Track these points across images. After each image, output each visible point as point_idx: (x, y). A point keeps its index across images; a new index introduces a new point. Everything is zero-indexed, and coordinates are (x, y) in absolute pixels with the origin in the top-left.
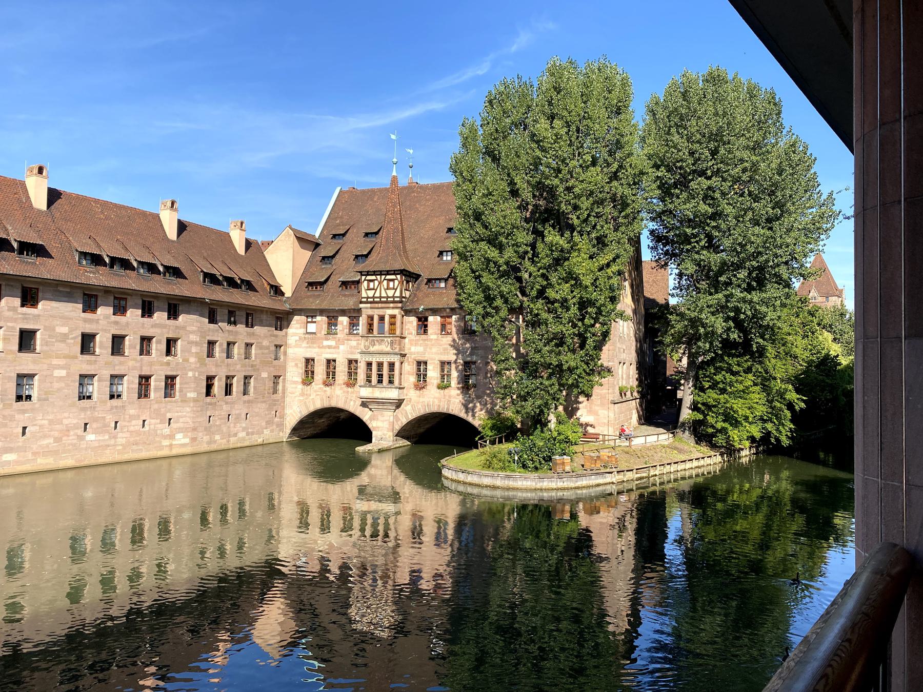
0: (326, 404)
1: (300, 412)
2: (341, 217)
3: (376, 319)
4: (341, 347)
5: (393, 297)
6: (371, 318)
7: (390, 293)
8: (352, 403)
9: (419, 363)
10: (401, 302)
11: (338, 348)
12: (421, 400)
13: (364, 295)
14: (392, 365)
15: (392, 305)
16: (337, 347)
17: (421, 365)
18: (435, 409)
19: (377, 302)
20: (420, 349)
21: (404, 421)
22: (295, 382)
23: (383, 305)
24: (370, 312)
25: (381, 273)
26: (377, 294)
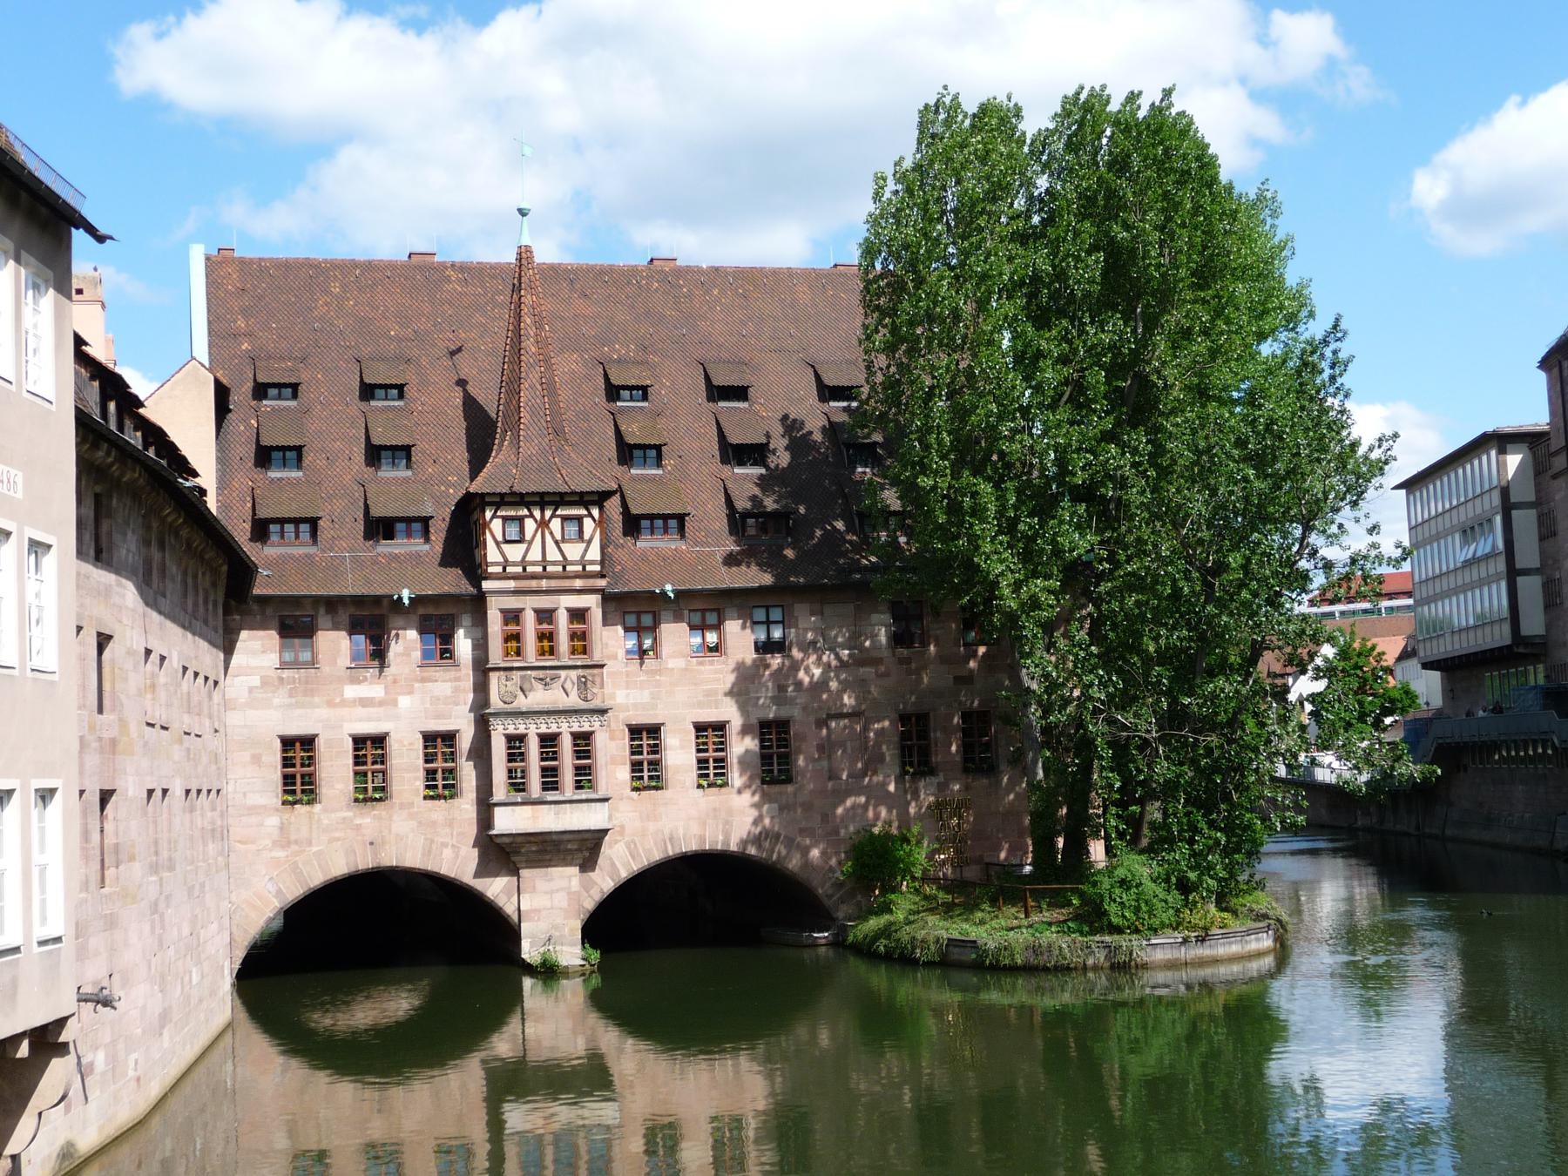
0: (365, 861)
1: (279, 892)
2: (249, 335)
3: (529, 619)
4: (404, 702)
6: (512, 616)
7: (573, 551)
8: (447, 853)
9: (635, 731)
10: (603, 576)
11: (395, 703)
12: (652, 827)
13: (492, 554)
14: (583, 741)
15: (578, 583)
16: (389, 702)
17: (645, 736)
18: (692, 846)
19: (534, 576)
20: (644, 696)
22: (253, 810)
23: (554, 584)
24: (512, 603)
25: (545, 500)
26: (535, 554)
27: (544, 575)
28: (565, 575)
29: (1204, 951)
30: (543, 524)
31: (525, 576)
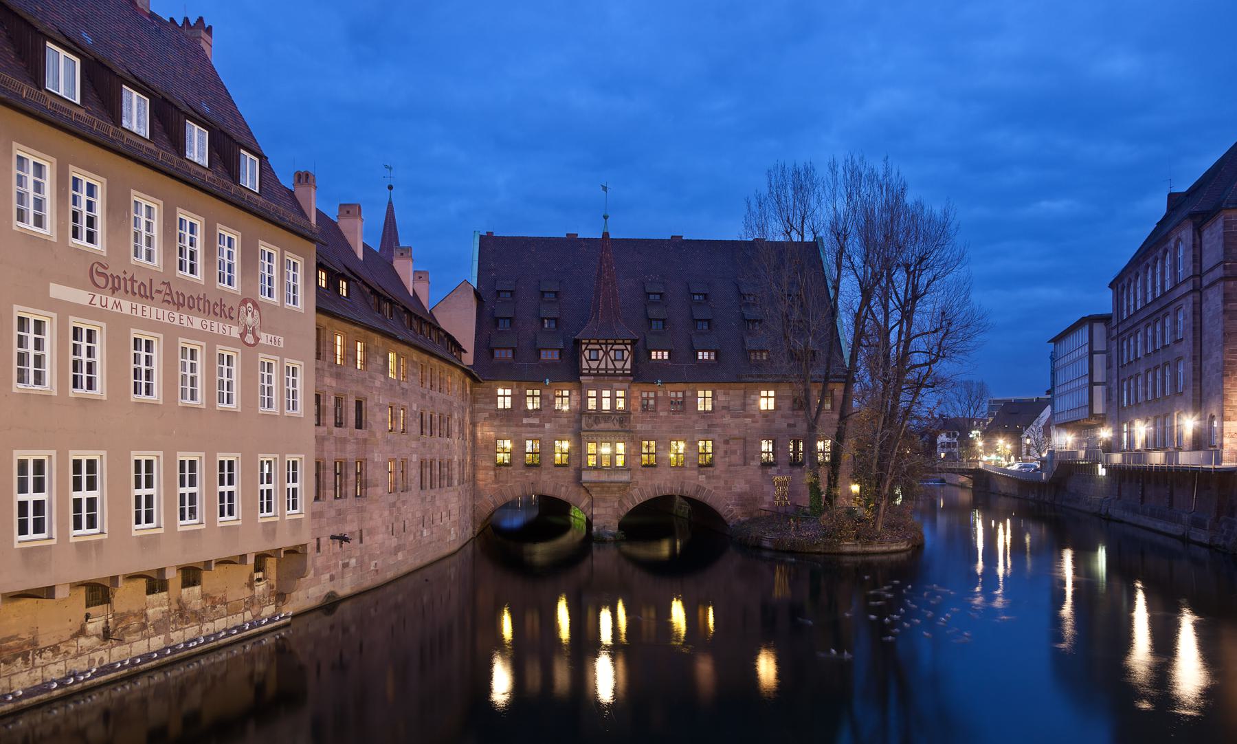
4: (547, 426)
5: (623, 369)
7: (619, 365)
8: (563, 489)
10: (630, 375)
13: (585, 365)
16: (541, 426)
21: (631, 506)
26: (603, 366)
27: (607, 374)
28: (615, 375)
29: (870, 549)
30: (606, 353)
31: (598, 375)
